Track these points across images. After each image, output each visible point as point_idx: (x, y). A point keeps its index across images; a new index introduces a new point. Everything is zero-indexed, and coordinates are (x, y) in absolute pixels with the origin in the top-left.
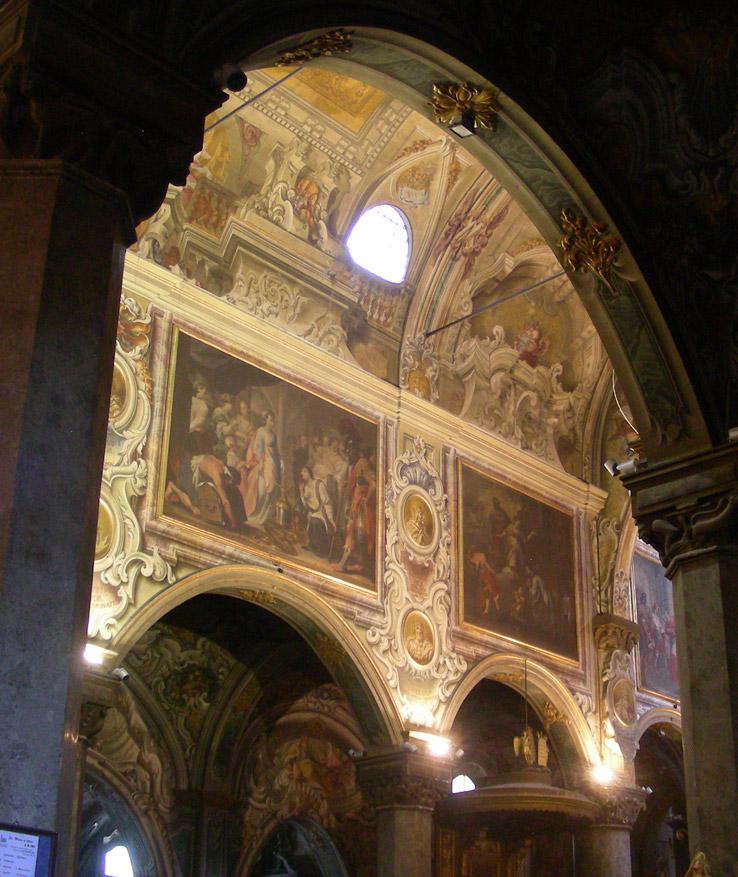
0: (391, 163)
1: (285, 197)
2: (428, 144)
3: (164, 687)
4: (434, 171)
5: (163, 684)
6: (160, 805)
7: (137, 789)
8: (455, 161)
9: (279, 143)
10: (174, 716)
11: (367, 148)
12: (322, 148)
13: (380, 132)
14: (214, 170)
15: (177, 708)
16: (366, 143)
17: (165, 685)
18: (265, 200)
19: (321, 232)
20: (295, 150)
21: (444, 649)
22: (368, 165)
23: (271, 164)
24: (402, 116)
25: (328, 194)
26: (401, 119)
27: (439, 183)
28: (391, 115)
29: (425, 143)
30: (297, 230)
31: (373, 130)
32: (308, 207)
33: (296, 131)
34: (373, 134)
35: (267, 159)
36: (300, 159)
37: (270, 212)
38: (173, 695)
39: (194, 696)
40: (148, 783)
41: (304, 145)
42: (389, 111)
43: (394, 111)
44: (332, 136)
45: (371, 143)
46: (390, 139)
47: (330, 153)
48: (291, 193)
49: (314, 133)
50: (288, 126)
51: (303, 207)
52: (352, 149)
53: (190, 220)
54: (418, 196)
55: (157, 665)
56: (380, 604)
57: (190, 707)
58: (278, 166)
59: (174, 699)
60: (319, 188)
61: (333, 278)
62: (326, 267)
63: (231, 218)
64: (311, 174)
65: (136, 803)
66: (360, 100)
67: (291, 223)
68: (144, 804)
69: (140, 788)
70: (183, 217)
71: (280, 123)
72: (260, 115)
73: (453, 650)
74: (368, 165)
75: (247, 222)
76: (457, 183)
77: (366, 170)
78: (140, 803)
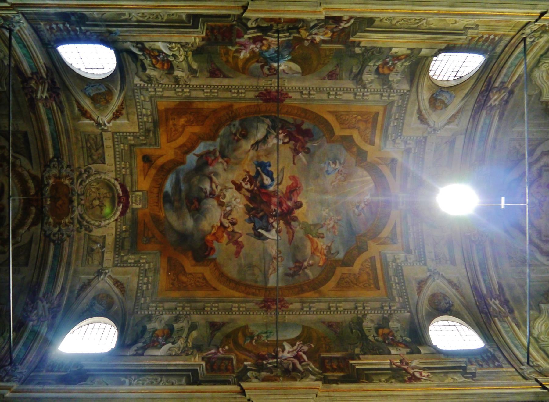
0: (124, 98)
1: (174, 55)
2: (113, 118)
4: (95, 107)
8: (91, 118)
9: (198, 77)
11: (145, 98)
12: (170, 86)
13: (145, 108)
14: (228, 51)
16: (147, 100)
18: (186, 50)
19: (137, 49)
20: (185, 78)
22: (136, 91)
23: (195, 66)
24: (141, 122)
25: (148, 67)
26: (140, 120)
27: (87, 104)
28: (148, 119)
29: (117, 115)
30: (154, 45)
31: (150, 107)
32: (156, 57)
33: (191, 86)
34: (148, 105)
35: (198, 68)
36: (179, 75)
37: (179, 46)
41: (182, 82)
42: (150, 120)
43: (148, 122)
44: (171, 93)
45: (145, 101)
46: (137, 109)
47: (164, 86)
48: (171, 59)
49: (180, 90)
50: (198, 86)
51: (159, 56)
52: (153, 94)
53: (232, 26)
54: (92, 91)
58: (190, 67)
60: (156, 68)
61: (111, 33)
62: (119, 35)
63: (204, 35)
64: (166, 72)
66: (170, 117)
67: (160, 46)
70: (238, 26)
71: (204, 86)
72: (217, 84)
74: (136, 91)
75: (192, 36)
76: (76, 109)
77: (135, 88)
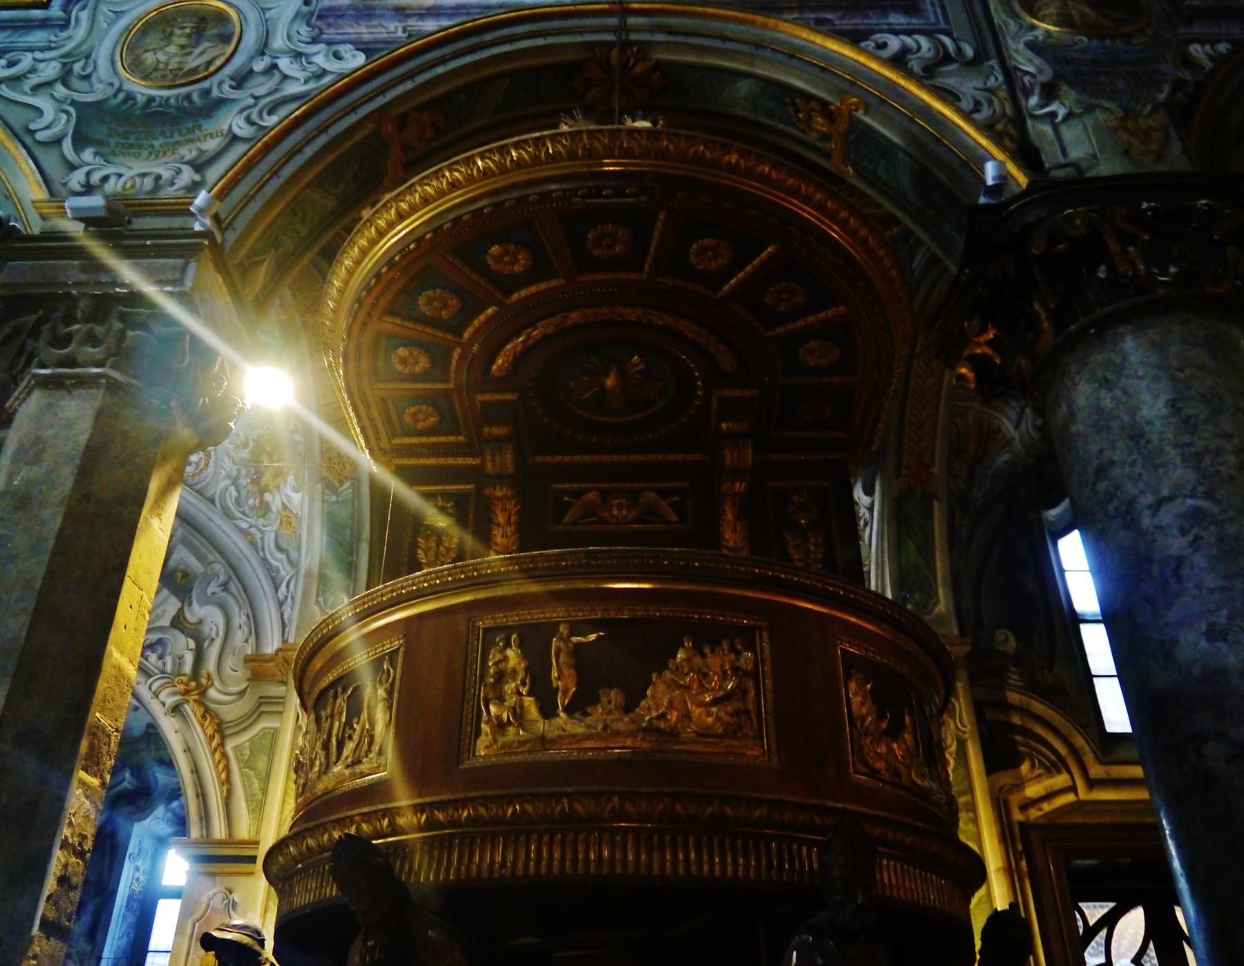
3: (234, 494)
5: (232, 489)
6: (212, 693)
7: (163, 672)
10: (259, 535)
15: (261, 521)
17: (237, 490)
21: (278, 42)
38: (251, 501)
39: (278, 487)
40: (189, 658)
55: (216, 462)
56: (61, 14)
57: (278, 512)
59: (252, 508)
65: (156, 695)
68: (174, 694)
69: (169, 668)
73: (315, 41)
78: (162, 696)
